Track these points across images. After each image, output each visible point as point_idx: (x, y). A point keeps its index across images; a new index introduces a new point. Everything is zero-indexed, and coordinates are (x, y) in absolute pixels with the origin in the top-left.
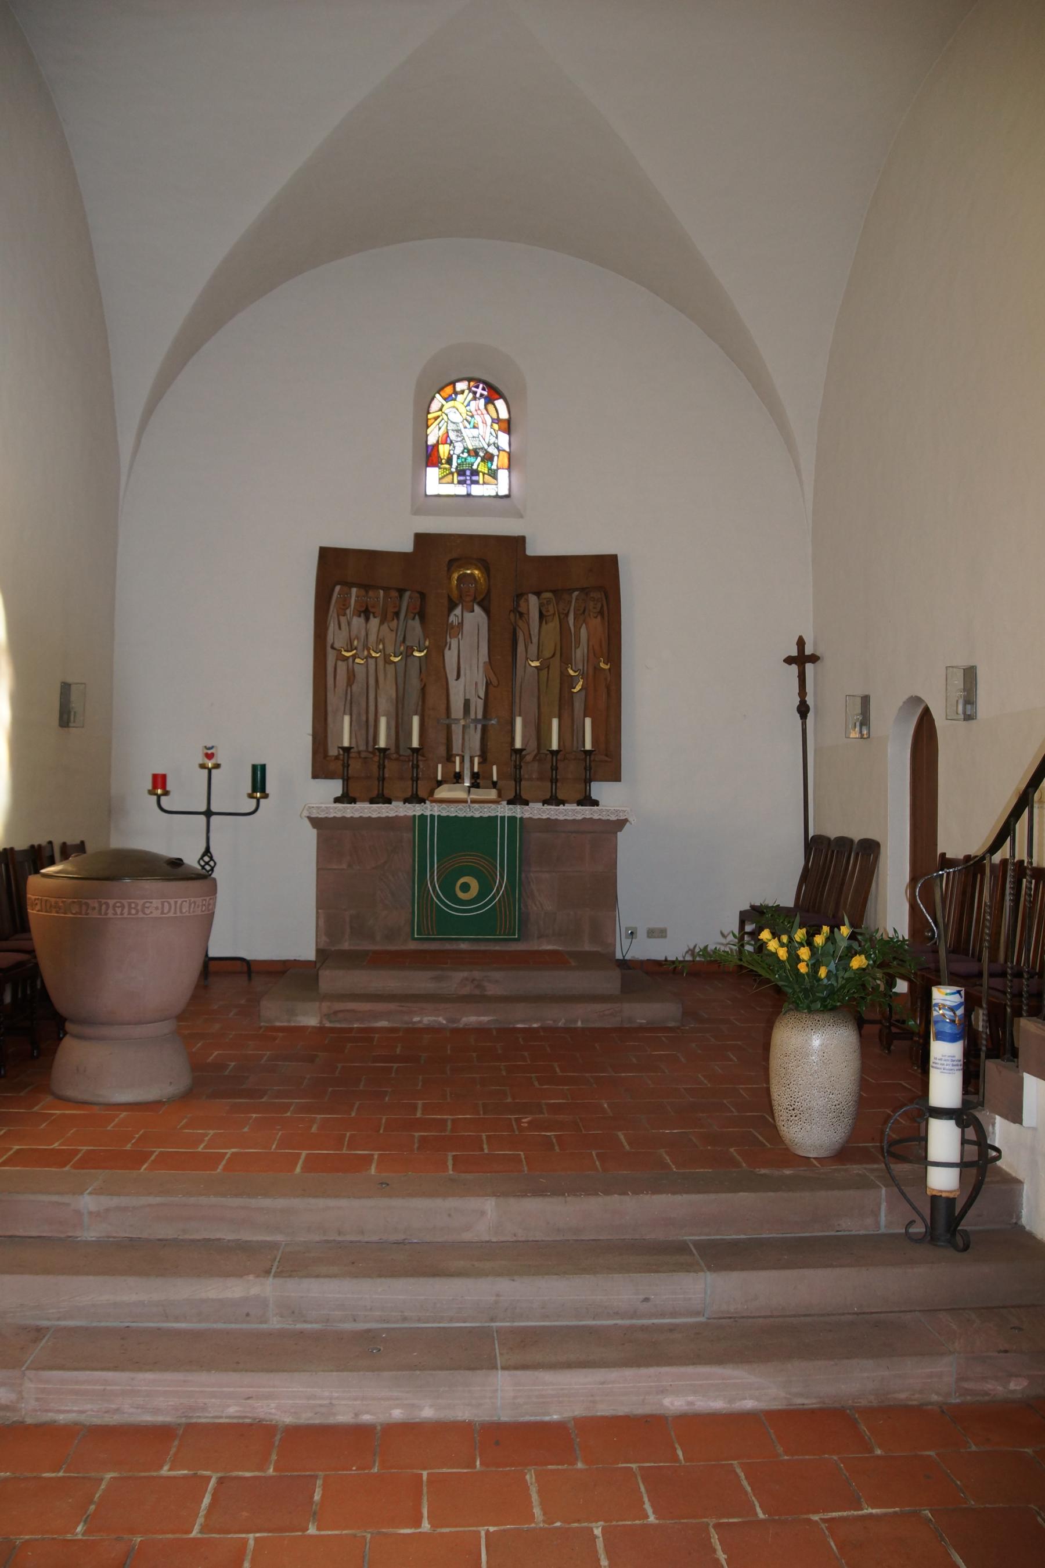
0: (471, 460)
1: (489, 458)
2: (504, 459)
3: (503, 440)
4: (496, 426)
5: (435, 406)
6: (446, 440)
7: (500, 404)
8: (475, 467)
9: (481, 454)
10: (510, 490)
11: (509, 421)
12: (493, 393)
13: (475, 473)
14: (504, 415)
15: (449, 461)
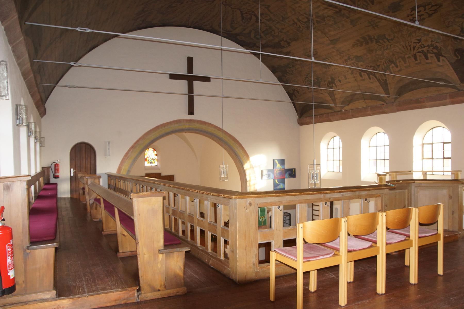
0: (151, 160)
1: (154, 160)
2: (156, 159)
3: (156, 157)
4: (155, 155)
5: (146, 152)
6: (148, 157)
7: (155, 152)
8: (152, 161)
9: (153, 159)
10: (157, 164)
11: (157, 154)
12: (155, 150)
13: (152, 162)
14: (156, 153)
15: (148, 161)
